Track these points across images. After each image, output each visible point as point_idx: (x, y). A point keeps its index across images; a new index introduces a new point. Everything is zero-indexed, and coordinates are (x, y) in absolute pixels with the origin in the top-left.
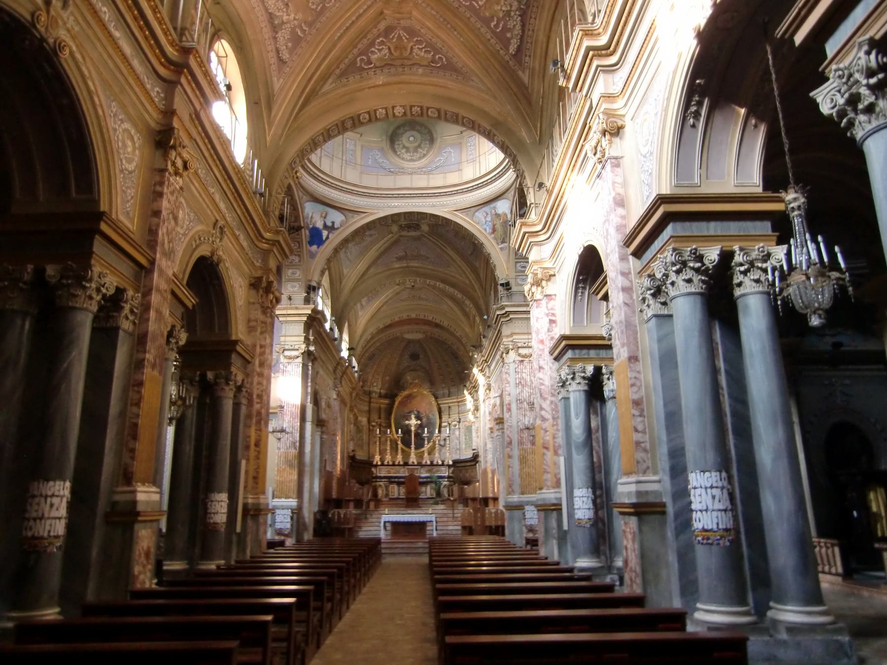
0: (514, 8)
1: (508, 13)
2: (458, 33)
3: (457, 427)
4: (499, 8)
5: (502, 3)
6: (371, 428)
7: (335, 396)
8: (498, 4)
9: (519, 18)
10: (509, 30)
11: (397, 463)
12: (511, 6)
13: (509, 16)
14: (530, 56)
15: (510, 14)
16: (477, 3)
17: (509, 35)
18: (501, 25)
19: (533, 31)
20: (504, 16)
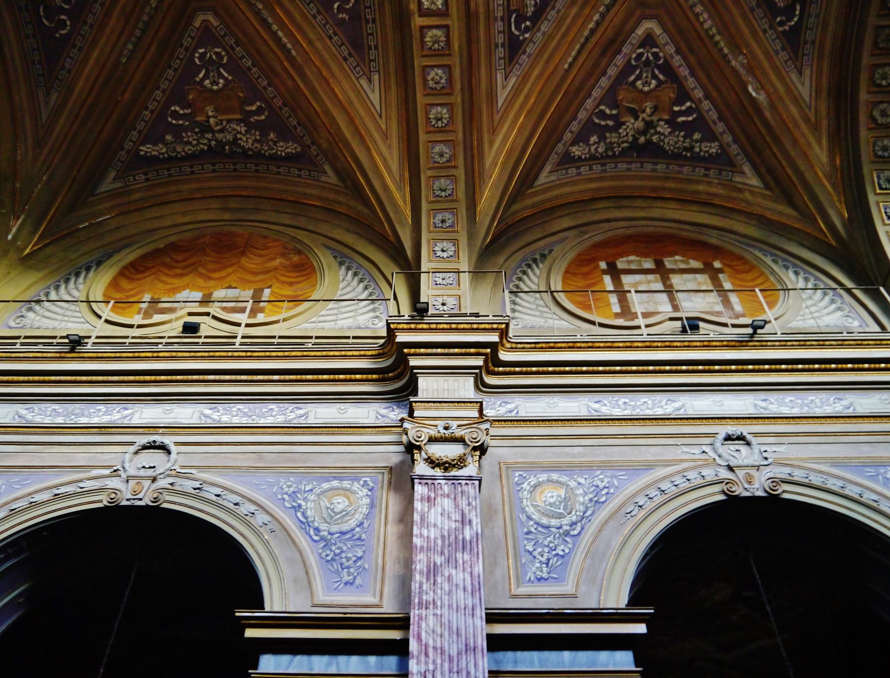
0: (219, 136)
1: (206, 128)
2: (132, 52)
4: (210, 114)
5: (220, 118)
8: (216, 110)
9: (206, 148)
10: (178, 138)
12: (221, 131)
13: (202, 132)
14: (147, 180)
15: (208, 133)
16: (206, 77)
17: (169, 138)
18: (181, 122)
19: (193, 173)
20: (199, 125)
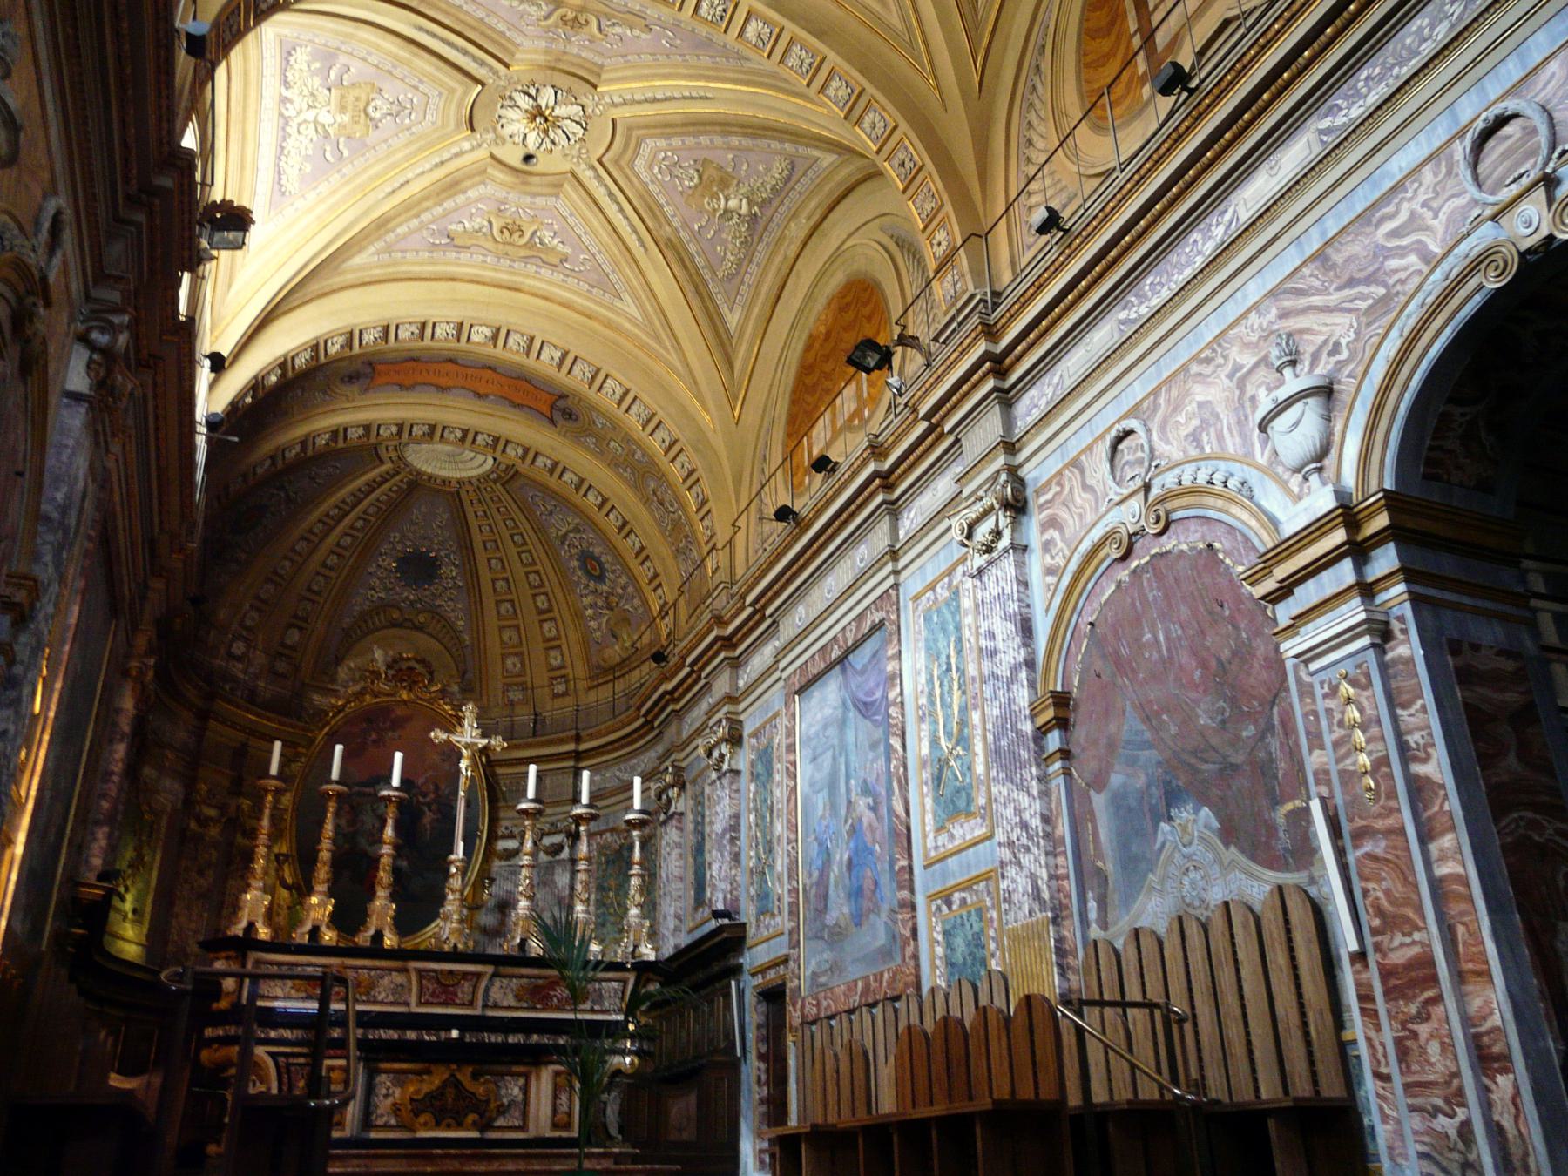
3: (565, 854)
6: (193, 825)
7: (77, 378)
11: (364, 938)
